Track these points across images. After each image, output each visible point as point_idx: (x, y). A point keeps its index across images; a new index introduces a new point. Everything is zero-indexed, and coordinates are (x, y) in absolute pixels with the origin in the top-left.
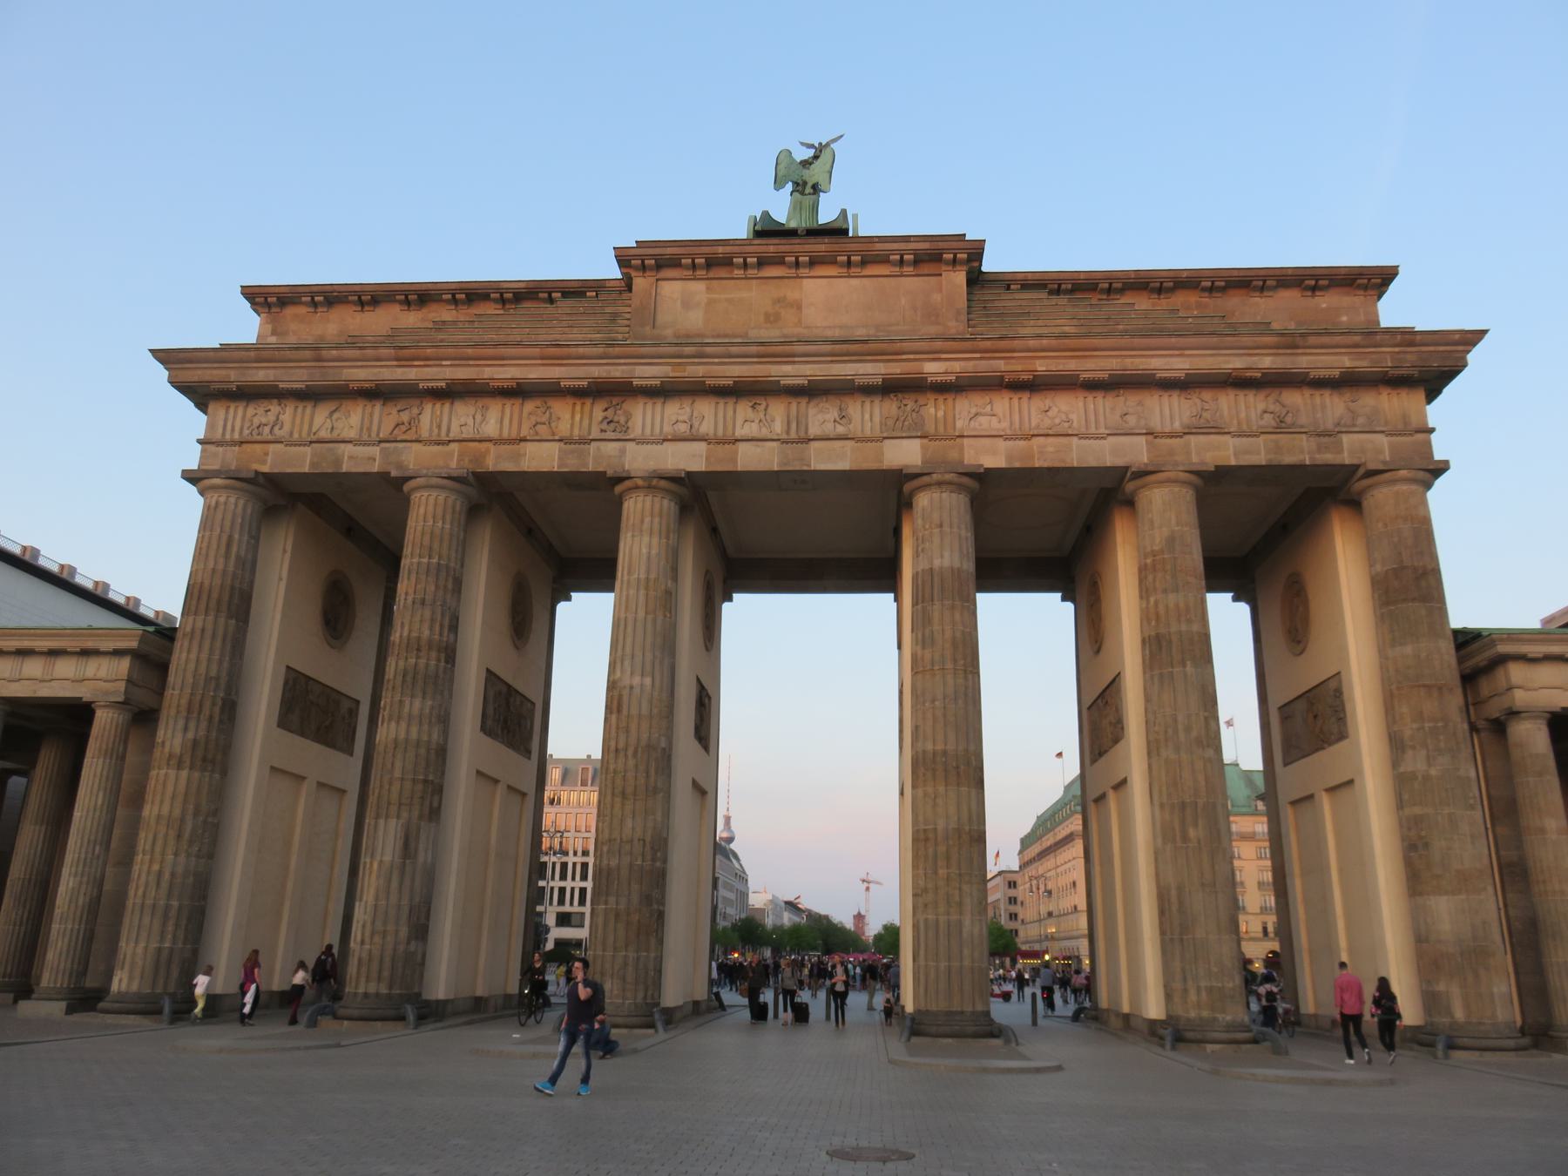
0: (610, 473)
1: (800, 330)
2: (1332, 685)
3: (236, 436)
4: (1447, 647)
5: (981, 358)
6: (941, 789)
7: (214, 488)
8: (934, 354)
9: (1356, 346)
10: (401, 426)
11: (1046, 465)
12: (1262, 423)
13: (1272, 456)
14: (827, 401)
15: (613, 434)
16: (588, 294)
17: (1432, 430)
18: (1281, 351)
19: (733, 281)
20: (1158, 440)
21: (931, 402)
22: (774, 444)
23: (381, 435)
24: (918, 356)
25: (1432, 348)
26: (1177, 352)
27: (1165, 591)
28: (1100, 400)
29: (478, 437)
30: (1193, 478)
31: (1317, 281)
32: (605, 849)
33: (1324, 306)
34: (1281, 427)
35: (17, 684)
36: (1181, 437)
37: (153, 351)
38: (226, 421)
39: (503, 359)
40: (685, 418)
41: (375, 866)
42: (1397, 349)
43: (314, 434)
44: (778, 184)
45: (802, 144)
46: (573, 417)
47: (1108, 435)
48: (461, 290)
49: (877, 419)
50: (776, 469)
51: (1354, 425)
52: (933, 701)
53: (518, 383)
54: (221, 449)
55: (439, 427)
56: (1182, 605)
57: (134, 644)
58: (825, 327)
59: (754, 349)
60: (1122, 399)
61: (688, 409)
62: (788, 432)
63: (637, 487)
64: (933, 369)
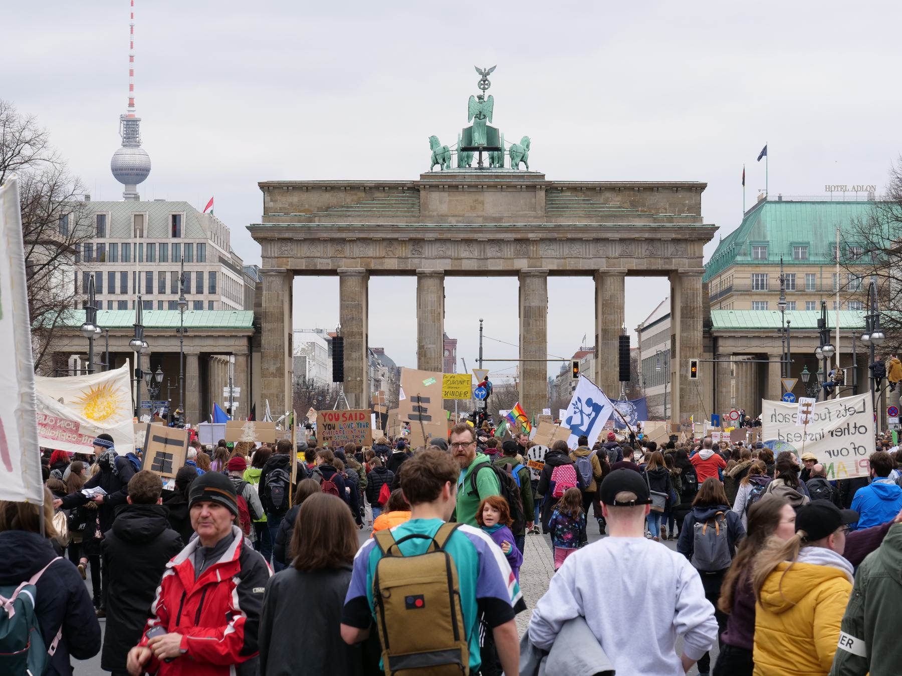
0: (418, 270)
3: (276, 255)
7: (271, 275)
8: (532, 231)
11: (571, 268)
12: (647, 254)
22: (476, 260)
27: (608, 314)
28: (591, 245)
29: (367, 256)
30: (621, 274)
34: (652, 256)
35: (206, 347)
37: (247, 227)
38: (271, 248)
44: (469, 119)
45: (478, 70)
46: (402, 249)
48: (348, 186)
49: (512, 250)
50: (476, 269)
54: (270, 260)
55: (353, 252)
56: (613, 319)
57: (250, 334)
59: (469, 229)
62: (480, 255)
63: (427, 276)
64: (531, 236)
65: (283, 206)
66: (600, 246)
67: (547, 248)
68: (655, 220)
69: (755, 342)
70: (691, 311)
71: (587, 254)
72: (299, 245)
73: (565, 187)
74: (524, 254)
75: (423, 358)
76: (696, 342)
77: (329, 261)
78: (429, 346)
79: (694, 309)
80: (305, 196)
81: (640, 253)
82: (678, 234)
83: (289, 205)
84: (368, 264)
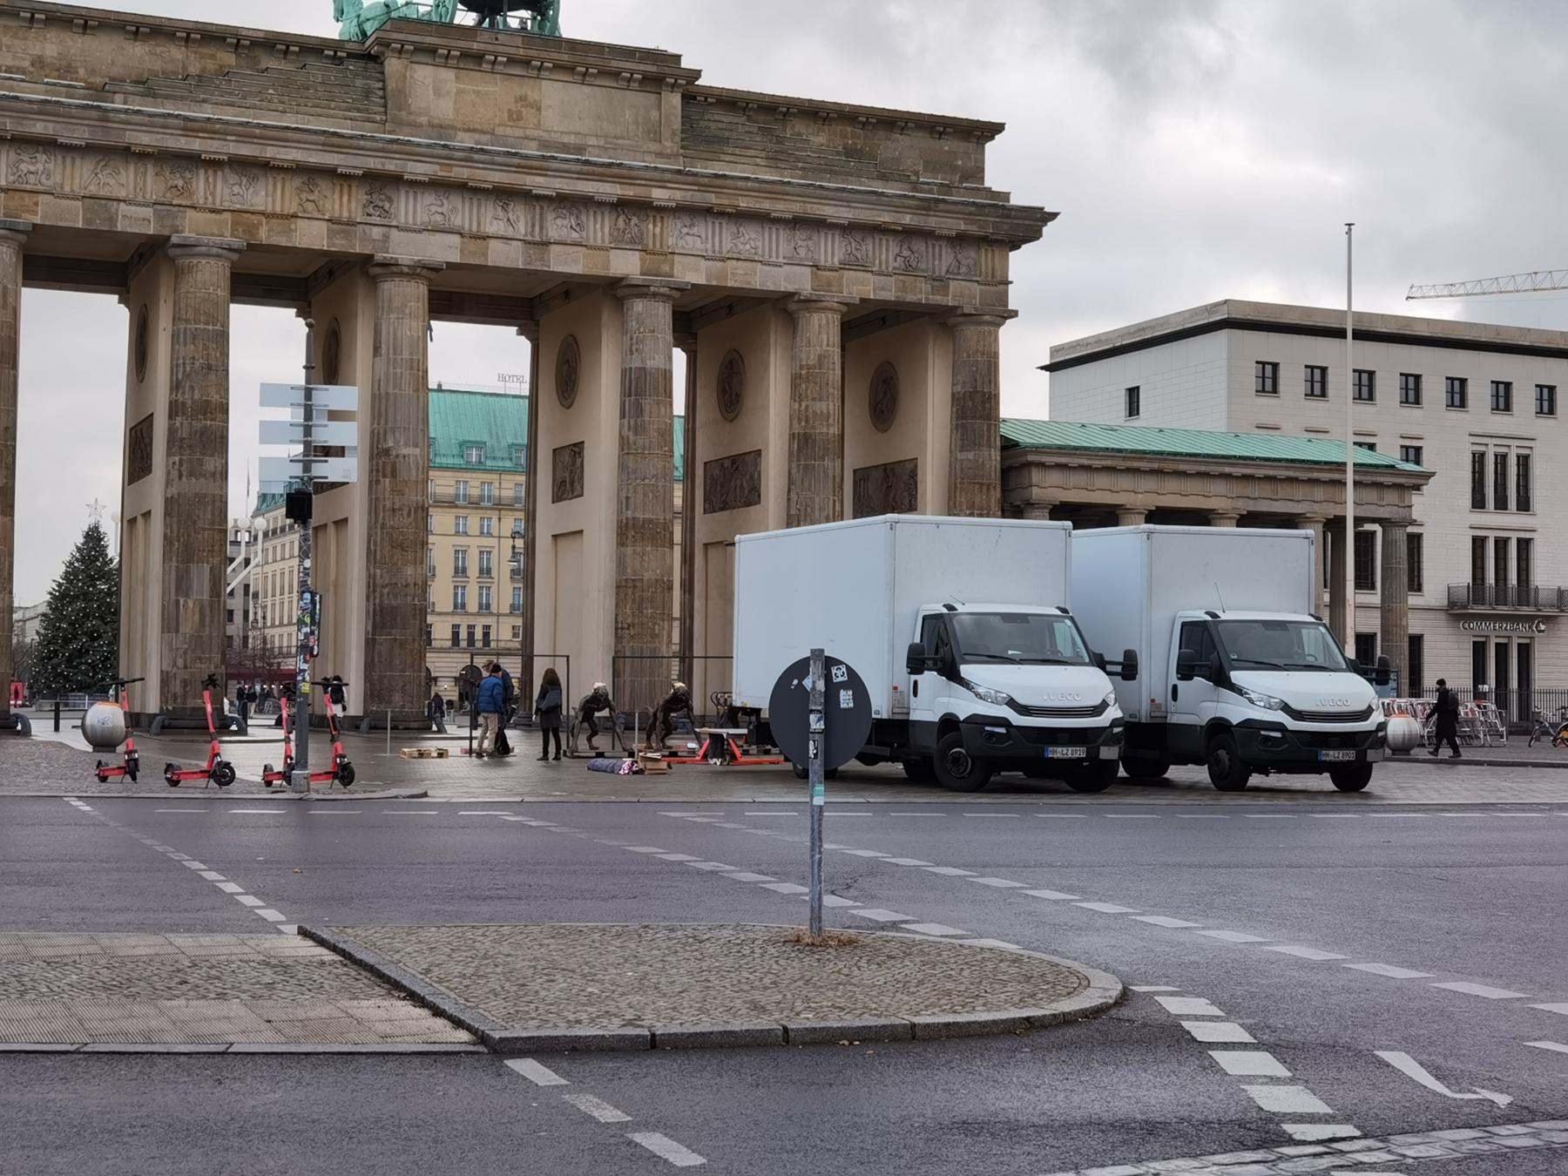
0: (379, 256)
1: (537, 133)
4: (996, 455)
5: (698, 191)
6: (649, 549)
9: (970, 214)
10: (174, 190)
12: (896, 265)
14: (564, 208)
15: (378, 219)
16: (326, 52)
17: (1011, 282)
18: (919, 212)
19: (480, 74)
20: (819, 272)
21: (651, 219)
22: (519, 243)
23: (154, 197)
24: (649, 183)
25: (1021, 222)
26: (845, 204)
27: (814, 399)
28: (781, 232)
29: (251, 209)
31: (945, 128)
32: (386, 591)
33: (946, 148)
34: (908, 269)
39: (287, 141)
40: (444, 209)
41: (191, 604)
43: (85, 188)
48: (197, 31)
49: (607, 230)
51: (959, 274)
52: (643, 480)
53: (297, 165)
55: (213, 194)
56: (825, 411)
58: (562, 133)
59: (516, 161)
60: (798, 233)
61: (445, 201)
63: (402, 274)
64: (659, 195)
65: (17, 63)
66: (800, 236)
67: (685, 230)
68: (915, 189)
69: (1102, 480)
70: (983, 402)
71: (774, 255)
72: (69, 160)
73: (712, 96)
74: (633, 241)
75: (387, 480)
76: (993, 474)
77: (149, 212)
78: (404, 451)
79: (990, 398)
80: (77, 45)
81: (884, 263)
82: (973, 222)
83: (32, 65)
84: (252, 229)
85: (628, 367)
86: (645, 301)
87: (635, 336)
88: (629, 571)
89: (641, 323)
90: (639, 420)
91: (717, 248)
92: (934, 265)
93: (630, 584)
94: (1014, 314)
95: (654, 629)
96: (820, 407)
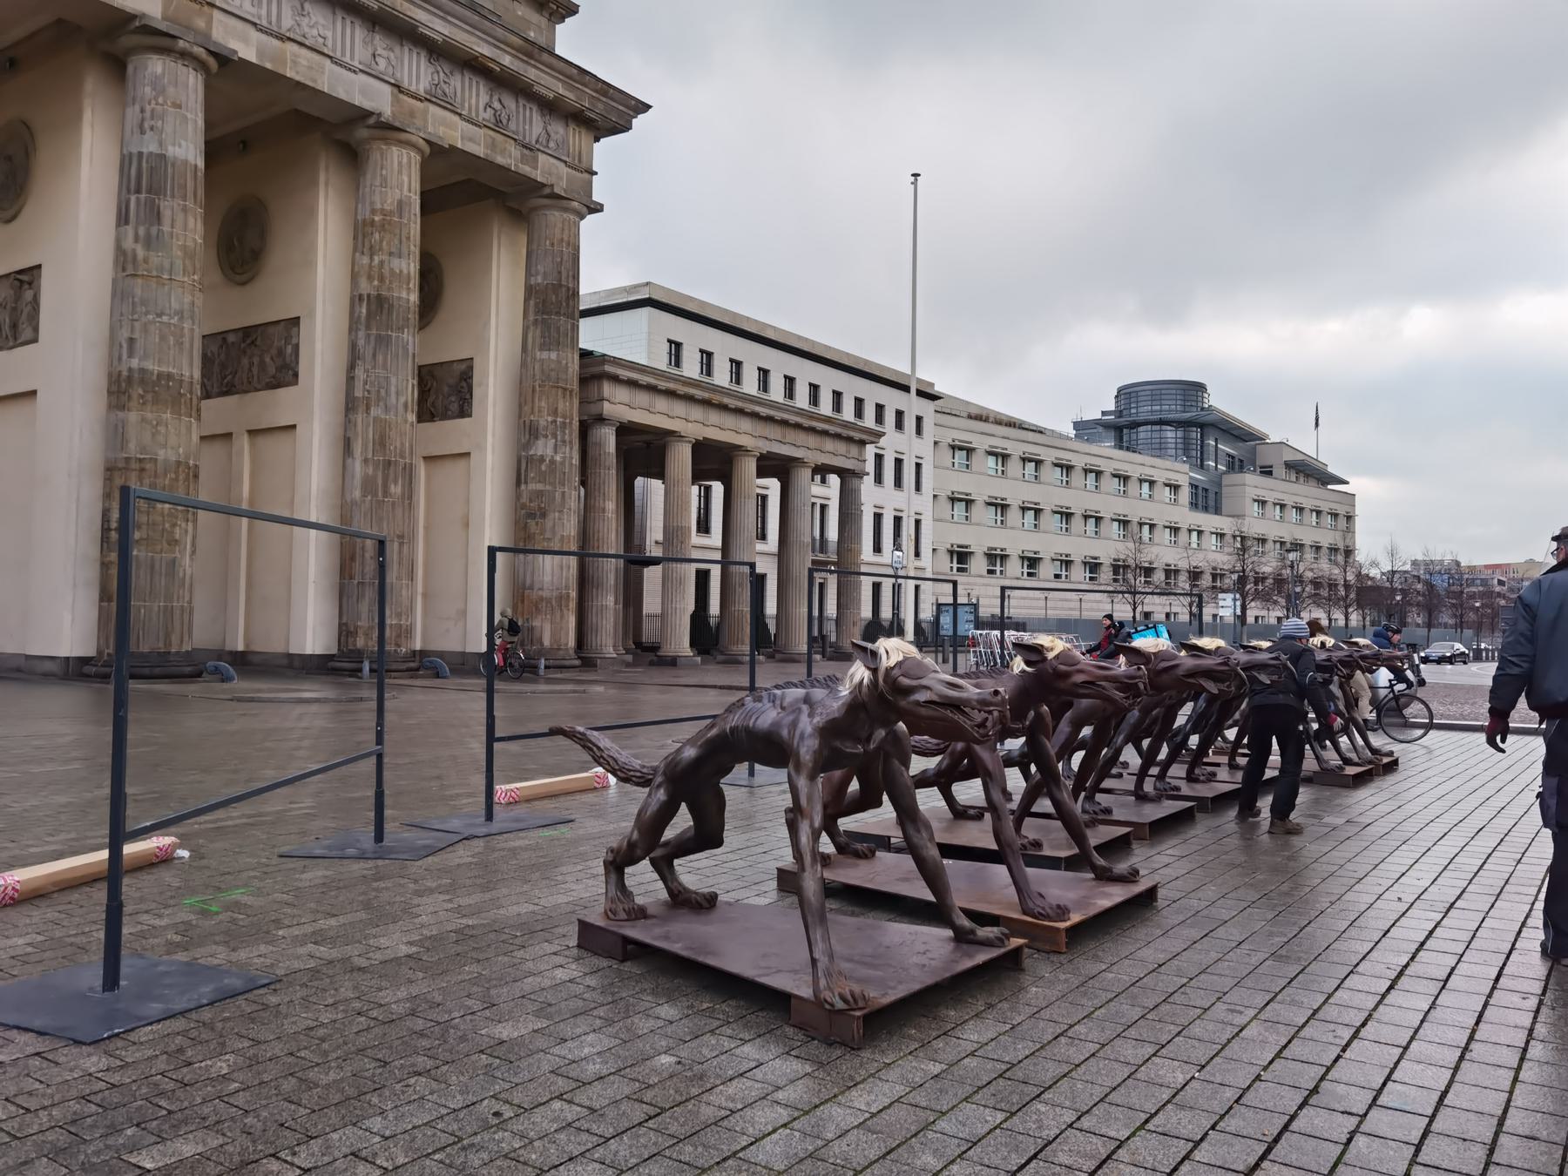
2: (463, 367)
11: (297, 78)
13: (489, 152)
20: (401, 96)
34: (498, 125)
36: (420, 100)
42: (594, 94)
47: (361, 71)
52: (160, 315)
56: (405, 271)
66: (380, 42)
69: (662, 404)
85: (134, 150)
86: (168, 60)
87: (148, 108)
88: (132, 446)
89: (160, 90)
90: (154, 230)
91: (274, 19)
92: (524, 129)
93: (134, 465)
94: (597, 208)
95: (172, 532)
96: (397, 264)
